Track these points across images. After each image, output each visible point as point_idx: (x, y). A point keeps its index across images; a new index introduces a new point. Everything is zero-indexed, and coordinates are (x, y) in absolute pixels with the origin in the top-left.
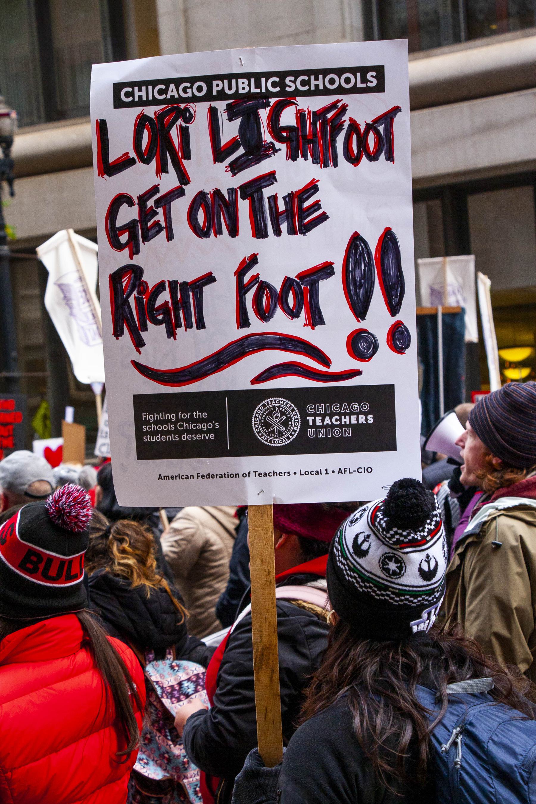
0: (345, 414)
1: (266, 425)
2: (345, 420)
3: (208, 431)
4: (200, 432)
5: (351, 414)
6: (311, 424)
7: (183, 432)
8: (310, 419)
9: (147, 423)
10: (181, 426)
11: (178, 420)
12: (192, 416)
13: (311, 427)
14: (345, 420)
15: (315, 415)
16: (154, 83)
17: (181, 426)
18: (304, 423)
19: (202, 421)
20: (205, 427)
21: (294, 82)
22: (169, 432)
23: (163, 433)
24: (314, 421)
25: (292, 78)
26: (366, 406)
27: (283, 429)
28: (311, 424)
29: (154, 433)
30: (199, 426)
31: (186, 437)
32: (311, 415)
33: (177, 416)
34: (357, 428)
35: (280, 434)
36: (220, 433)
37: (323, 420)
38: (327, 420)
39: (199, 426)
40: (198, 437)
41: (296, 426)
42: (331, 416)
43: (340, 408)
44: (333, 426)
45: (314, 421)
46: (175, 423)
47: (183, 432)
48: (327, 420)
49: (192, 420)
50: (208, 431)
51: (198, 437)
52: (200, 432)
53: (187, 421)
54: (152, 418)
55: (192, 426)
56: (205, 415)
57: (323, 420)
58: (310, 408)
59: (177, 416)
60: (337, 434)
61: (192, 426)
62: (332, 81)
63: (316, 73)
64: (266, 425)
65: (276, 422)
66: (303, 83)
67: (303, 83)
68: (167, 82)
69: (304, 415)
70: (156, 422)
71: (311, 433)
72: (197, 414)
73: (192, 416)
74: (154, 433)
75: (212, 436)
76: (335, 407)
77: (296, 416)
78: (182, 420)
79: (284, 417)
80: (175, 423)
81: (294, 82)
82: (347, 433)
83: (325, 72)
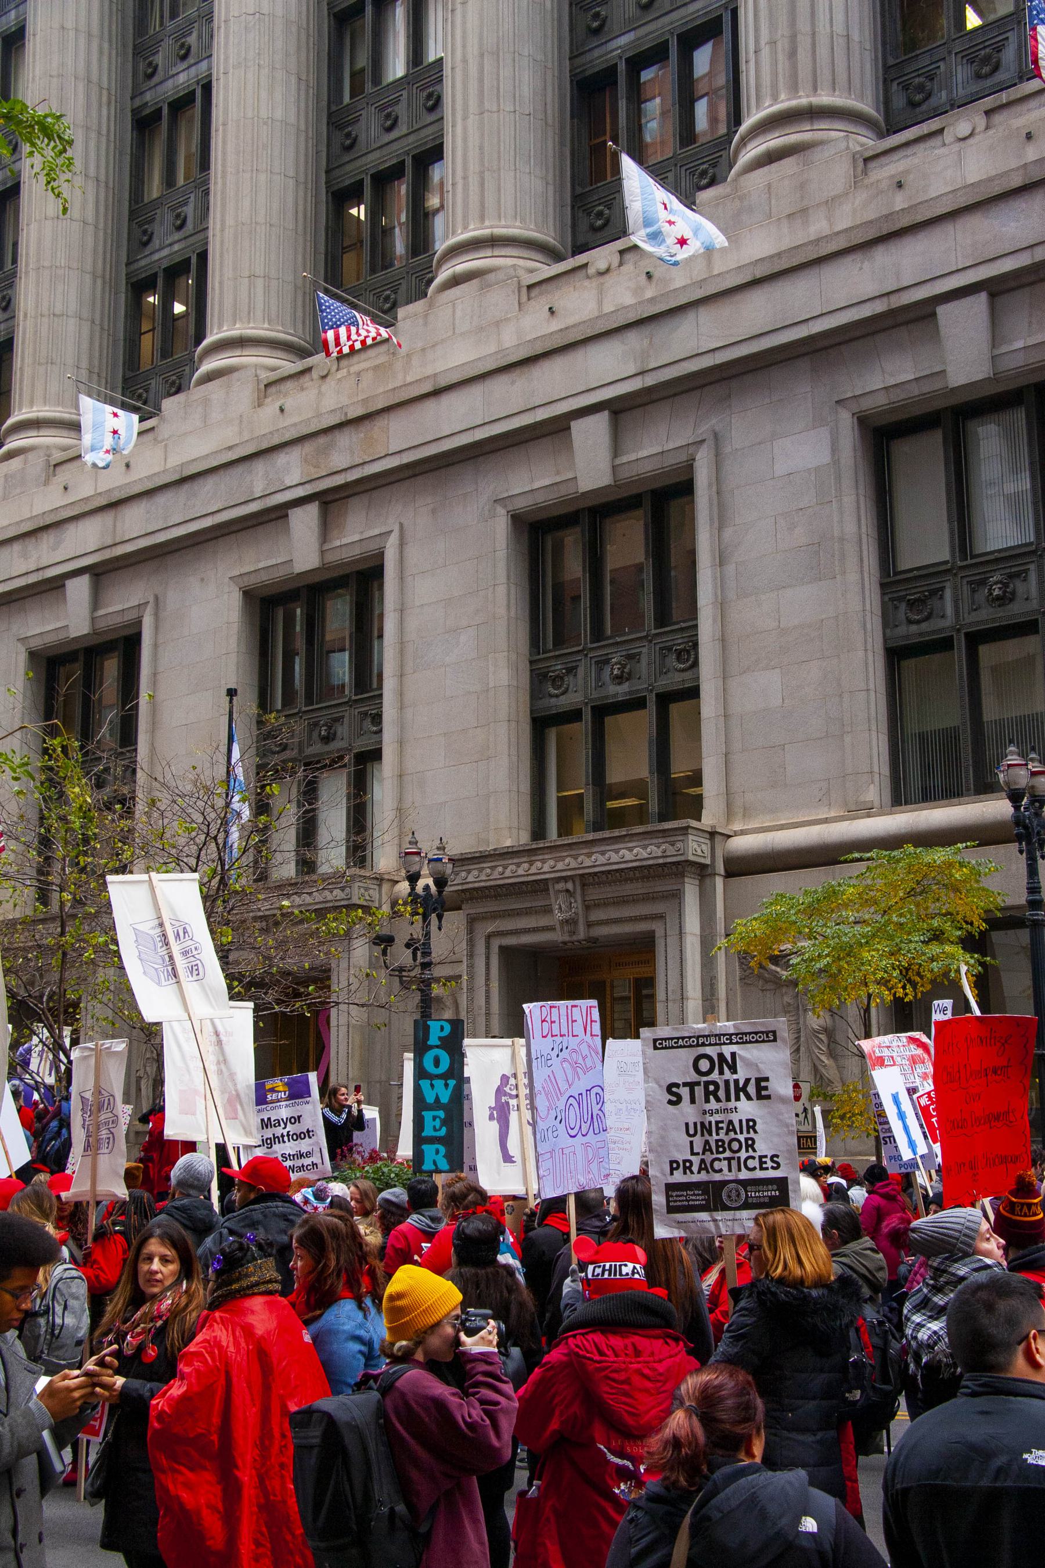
1: (729, 1197)
2: (765, 1194)
14: (765, 1194)
16: (672, 1039)
18: (747, 1195)
20: (701, 1198)
26: (775, 1187)
29: (675, 1201)
34: (771, 1197)
41: (743, 1196)
54: (674, 1194)
58: (749, 1188)
60: (762, 1200)
64: (729, 1197)
65: (734, 1194)
68: (678, 1038)
69: (746, 1192)
71: (750, 1200)
72: (696, 1192)
74: (675, 1201)
77: (743, 1192)
82: (767, 1200)
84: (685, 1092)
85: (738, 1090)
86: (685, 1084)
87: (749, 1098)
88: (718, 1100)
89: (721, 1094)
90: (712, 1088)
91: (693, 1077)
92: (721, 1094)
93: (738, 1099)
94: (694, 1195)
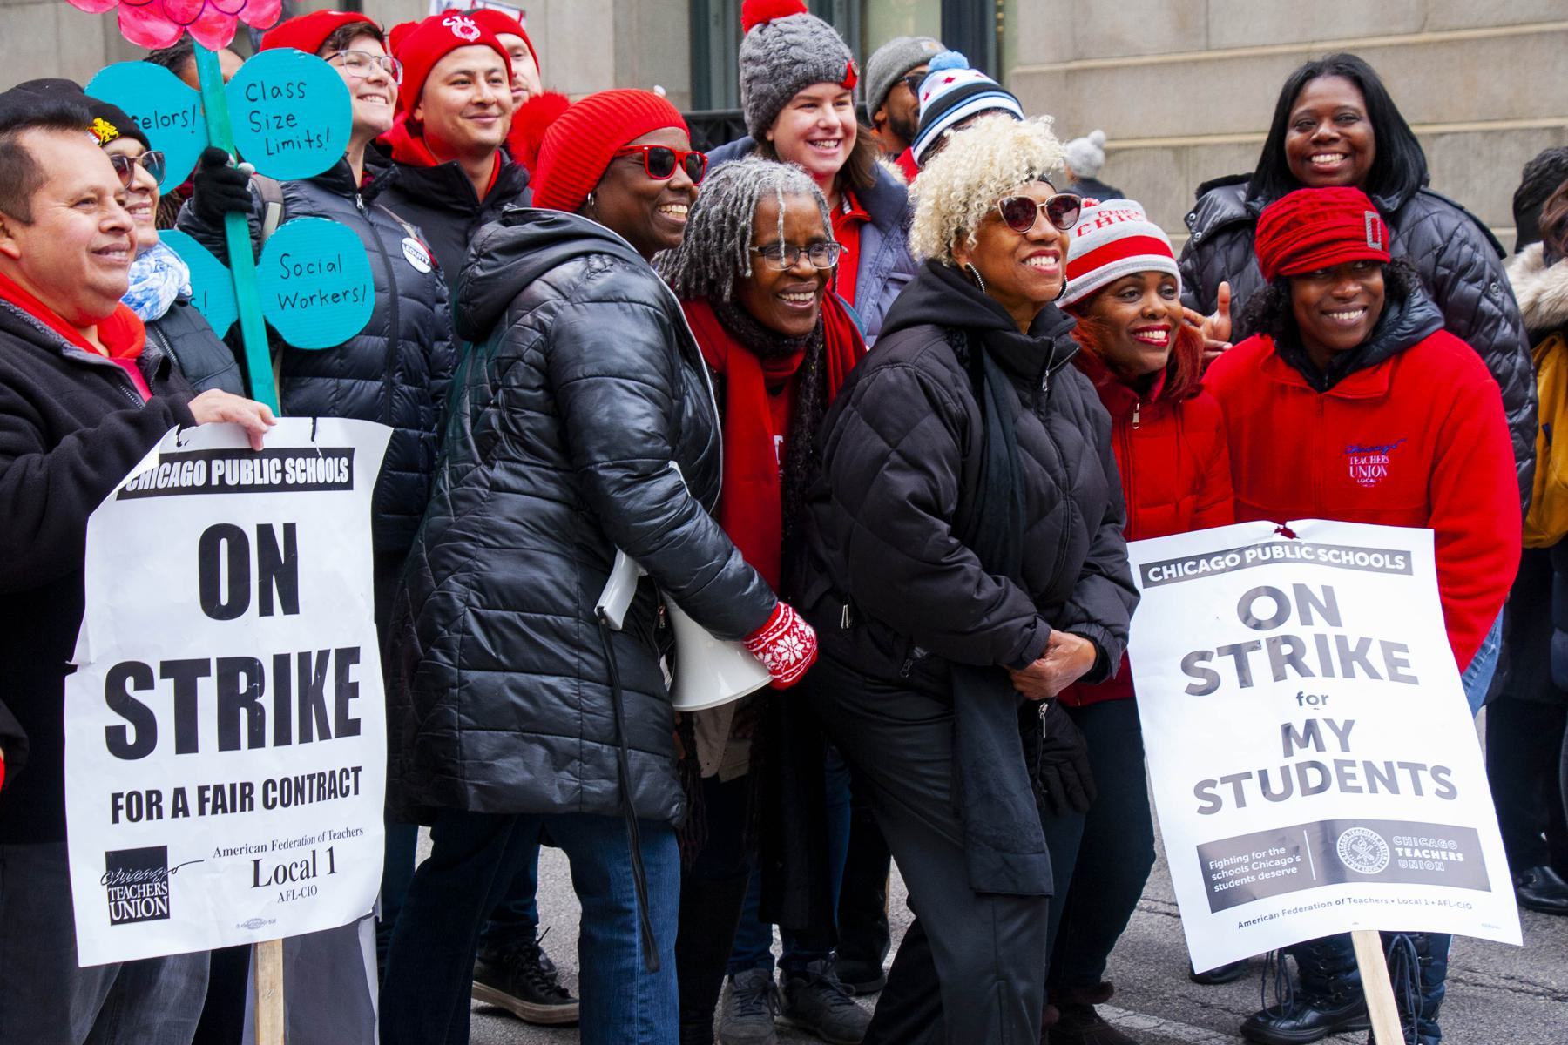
0: (1434, 849)
2: (1435, 855)
3: (1289, 866)
4: (1280, 867)
5: (1440, 849)
6: (1400, 854)
7: (1259, 872)
8: (1400, 850)
10: (1255, 866)
11: (1252, 861)
12: (1267, 854)
13: (1400, 858)
14: (1435, 855)
15: (1404, 847)
17: (1255, 866)
18: (1394, 855)
19: (1280, 857)
20: (1284, 862)
21: (1326, 554)
24: (1403, 852)
25: (1324, 551)
28: (1400, 854)
30: (1278, 863)
31: (1262, 876)
32: (1398, 847)
33: (1250, 857)
37: (1413, 853)
38: (1417, 853)
39: (1278, 863)
40: (1278, 873)
42: (1421, 849)
43: (1428, 842)
44: (1424, 859)
45: (1403, 852)
46: (1249, 864)
47: (1259, 872)
48: (1417, 853)
49: (1268, 858)
50: (1289, 866)
51: (1278, 873)
52: (1280, 867)
53: (1263, 860)
55: (1269, 864)
56: (1282, 851)
57: (1413, 853)
58: (1396, 840)
59: (1250, 857)
60: (1429, 866)
61: (1269, 864)
62: (1362, 559)
63: (1348, 549)
66: (1335, 557)
67: (1335, 557)
69: (1392, 847)
72: (1273, 852)
73: (1267, 854)
75: (1294, 870)
76: (1423, 841)
78: (1256, 860)
80: (1249, 864)
81: (1326, 554)
83: (1356, 550)
91: (1246, 635)
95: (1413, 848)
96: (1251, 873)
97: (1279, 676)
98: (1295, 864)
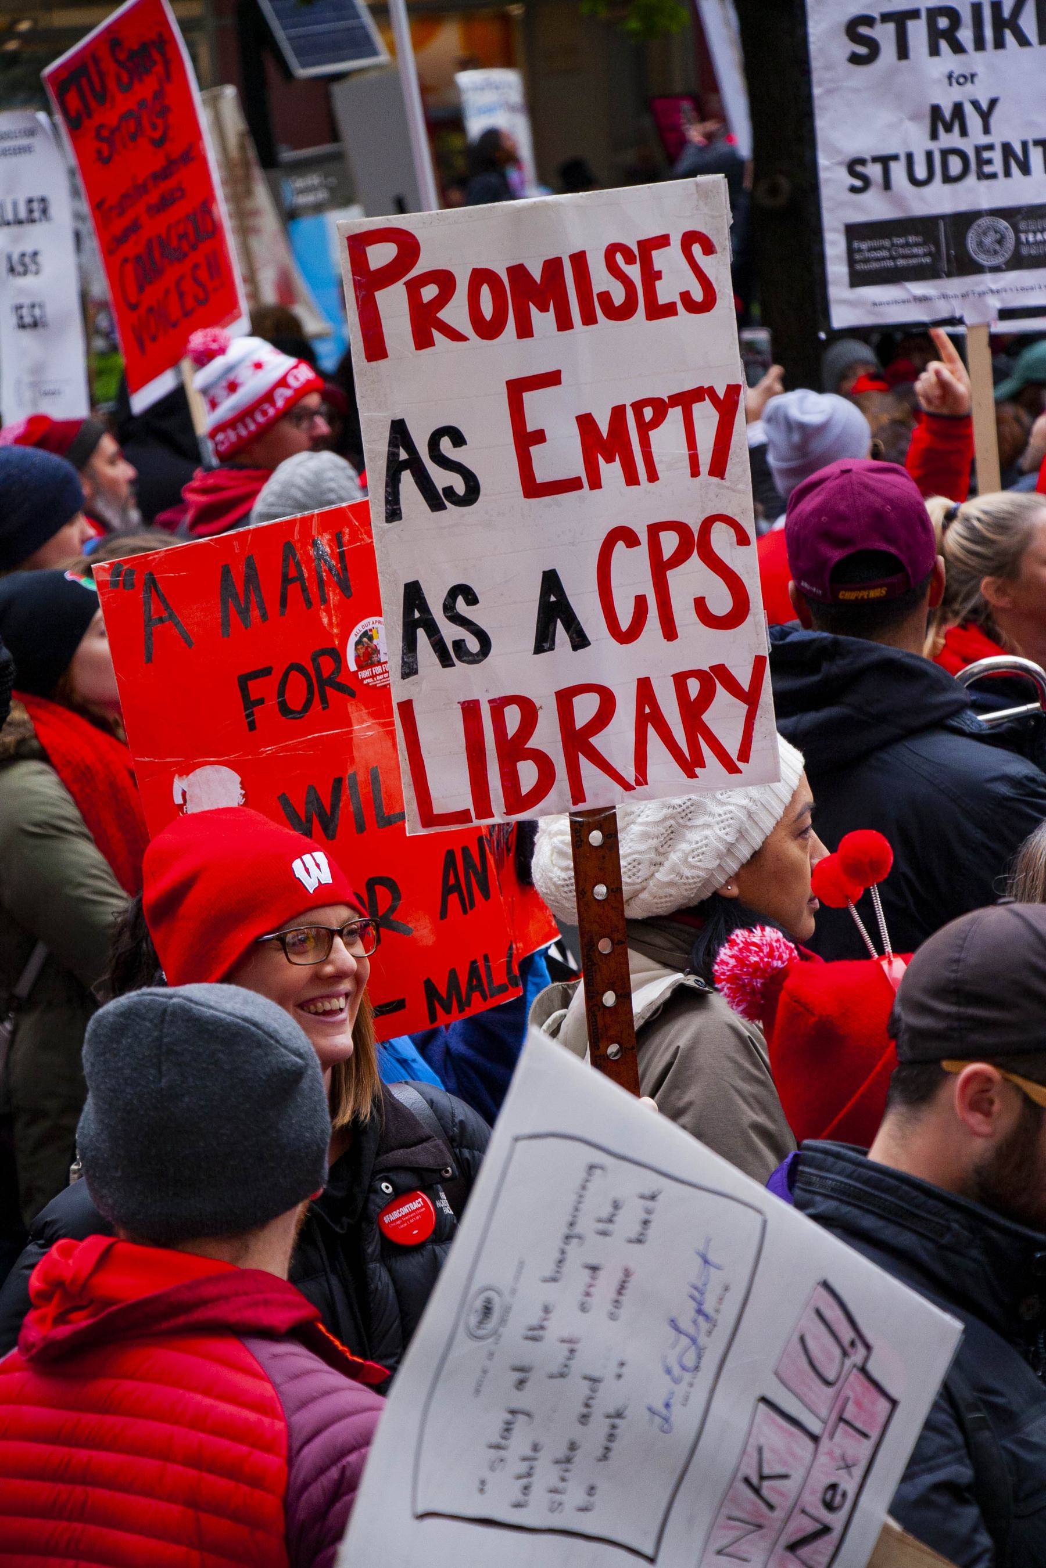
3: (925, 255)
8: (1023, 236)
9: (860, 250)
11: (893, 245)
15: (1026, 232)
19: (917, 245)
22: (883, 259)
23: (878, 260)
27: (997, 247)
29: (867, 261)
31: (901, 262)
32: (1022, 232)
35: (996, 252)
36: (936, 256)
50: (925, 255)
52: (916, 256)
53: (902, 246)
54: (864, 246)
55: (907, 251)
61: (907, 251)
64: (980, 244)
69: (1017, 231)
70: (870, 250)
71: (1025, 251)
72: (912, 239)
74: (867, 261)
77: (1010, 234)
79: (998, 236)
80: (889, 250)
84: (885, 34)
85: (1000, 24)
86: (886, 17)
87: (1023, 41)
88: (958, 48)
89: (965, 35)
90: (943, 23)
92: (965, 35)
93: (999, 44)
94: (907, 245)
95: (1035, 233)
96: (892, 258)
97: (934, 51)
98: (930, 254)
